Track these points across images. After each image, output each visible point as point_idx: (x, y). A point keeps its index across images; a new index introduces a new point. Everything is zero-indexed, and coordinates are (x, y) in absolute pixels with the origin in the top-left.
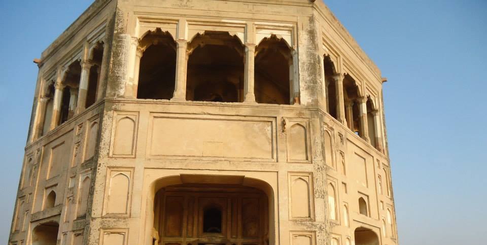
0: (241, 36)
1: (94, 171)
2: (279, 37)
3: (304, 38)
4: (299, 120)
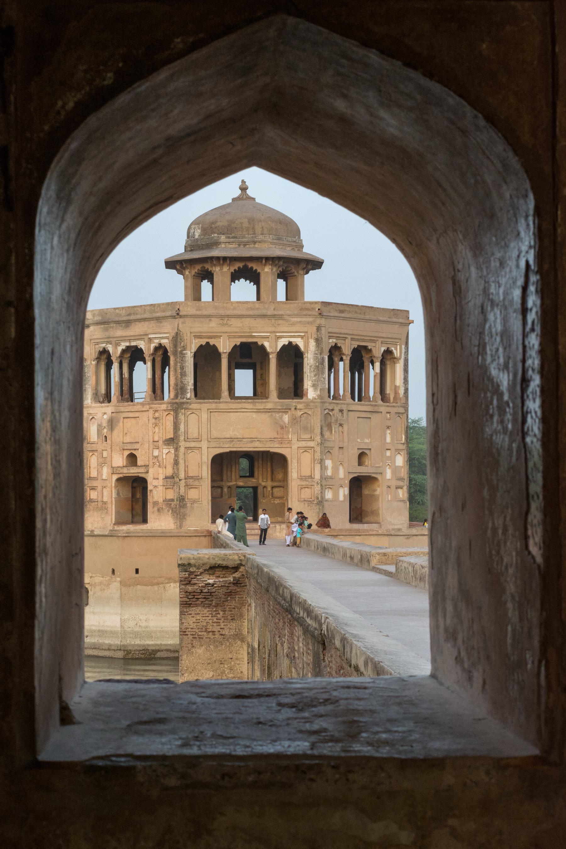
0: (267, 344)
1: (177, 449)
2: (294, 344)
3: (312, 344)
4: (306, 411)
